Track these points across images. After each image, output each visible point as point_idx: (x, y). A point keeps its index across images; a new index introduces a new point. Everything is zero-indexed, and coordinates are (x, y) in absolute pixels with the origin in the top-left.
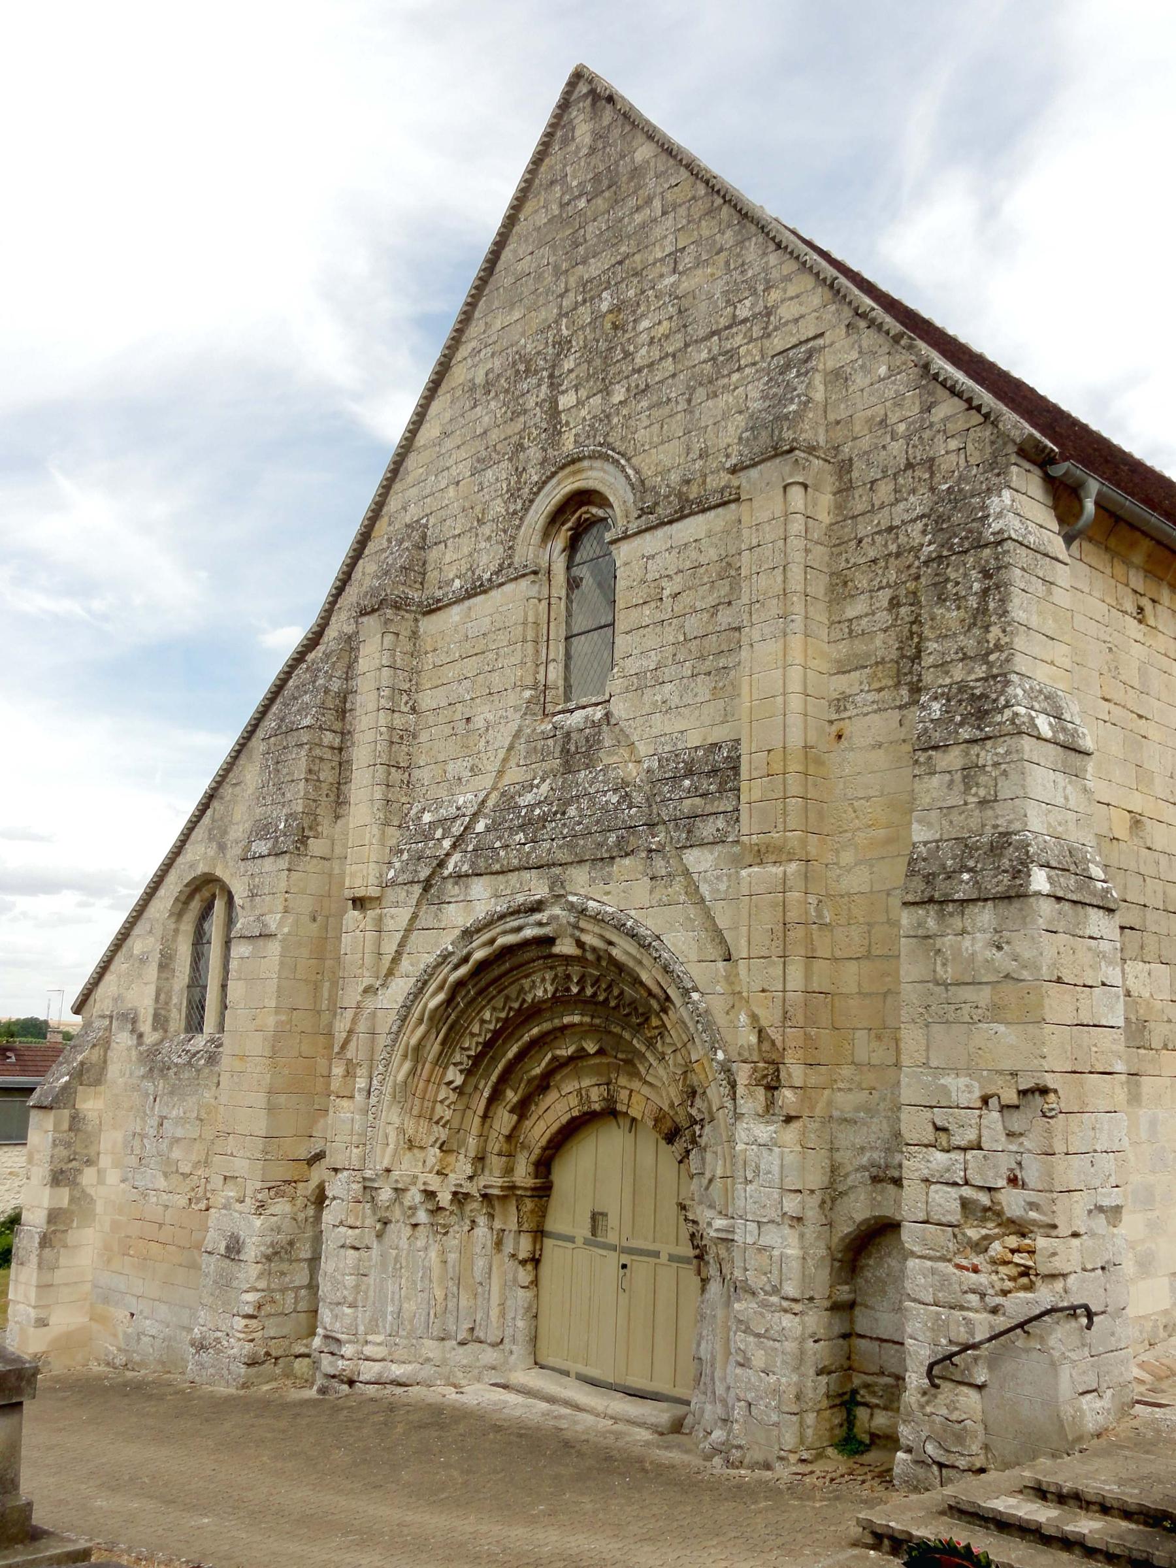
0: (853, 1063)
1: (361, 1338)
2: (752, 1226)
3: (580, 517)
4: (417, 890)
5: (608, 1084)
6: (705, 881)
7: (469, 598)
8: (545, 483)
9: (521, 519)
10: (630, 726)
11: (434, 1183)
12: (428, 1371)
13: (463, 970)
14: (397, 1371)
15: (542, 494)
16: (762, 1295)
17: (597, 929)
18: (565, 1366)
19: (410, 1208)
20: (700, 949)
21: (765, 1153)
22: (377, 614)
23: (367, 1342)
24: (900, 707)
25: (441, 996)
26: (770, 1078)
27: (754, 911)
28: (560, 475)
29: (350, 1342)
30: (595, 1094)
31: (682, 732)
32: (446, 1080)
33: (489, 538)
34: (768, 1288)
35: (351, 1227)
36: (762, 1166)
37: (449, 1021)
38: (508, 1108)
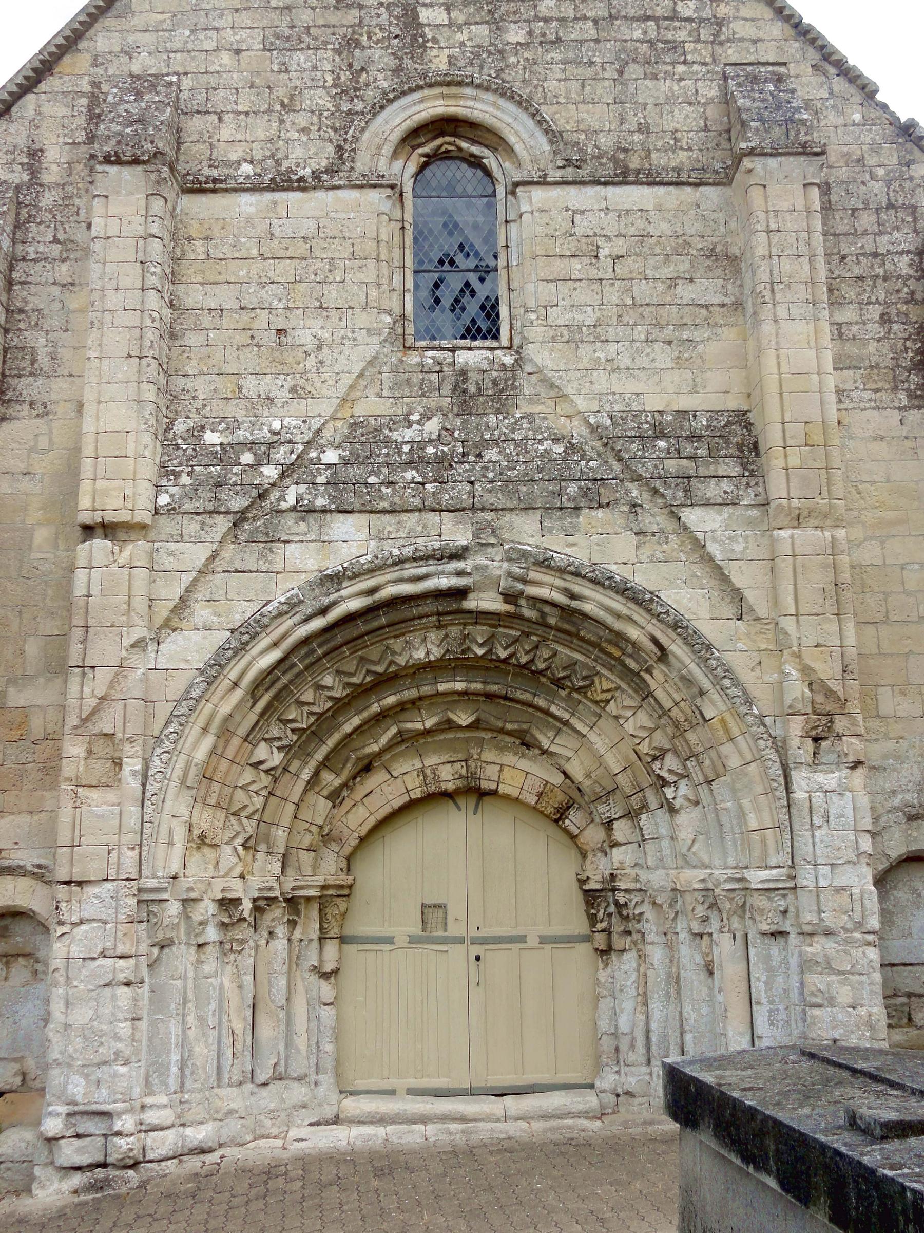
0: (879, 716)
1: (137, 1104)
3: (441, 146)
4: (223, 524)
5: (466, 761)
6: (714, 540)
7: (273, 190)
8: (404, 93)
9: (366, 123)
10: (561, 377)
11: (237, 889)
12: (233, 1127)
13: (318, 623)
14: (198, 1135)
15: (396, 105)
16: (844, 935)
17: (559, 582)
18: (385, 1085)
19: (201, 924)
20: (712, 606)
21: (835, 798)
22: (140, 168)
23: (143, 1107)
24: (899, 409)
25: (275, 655)
26: (820, 729)
28: (426, 92)
29: (125, 1112)
30: (446, 773)
31: (637, 394)
32: (254, 759)
33: (305, 130)
34: (849, 926)
35: (121, 957)
37: (278, 686)
38: (325, 793)
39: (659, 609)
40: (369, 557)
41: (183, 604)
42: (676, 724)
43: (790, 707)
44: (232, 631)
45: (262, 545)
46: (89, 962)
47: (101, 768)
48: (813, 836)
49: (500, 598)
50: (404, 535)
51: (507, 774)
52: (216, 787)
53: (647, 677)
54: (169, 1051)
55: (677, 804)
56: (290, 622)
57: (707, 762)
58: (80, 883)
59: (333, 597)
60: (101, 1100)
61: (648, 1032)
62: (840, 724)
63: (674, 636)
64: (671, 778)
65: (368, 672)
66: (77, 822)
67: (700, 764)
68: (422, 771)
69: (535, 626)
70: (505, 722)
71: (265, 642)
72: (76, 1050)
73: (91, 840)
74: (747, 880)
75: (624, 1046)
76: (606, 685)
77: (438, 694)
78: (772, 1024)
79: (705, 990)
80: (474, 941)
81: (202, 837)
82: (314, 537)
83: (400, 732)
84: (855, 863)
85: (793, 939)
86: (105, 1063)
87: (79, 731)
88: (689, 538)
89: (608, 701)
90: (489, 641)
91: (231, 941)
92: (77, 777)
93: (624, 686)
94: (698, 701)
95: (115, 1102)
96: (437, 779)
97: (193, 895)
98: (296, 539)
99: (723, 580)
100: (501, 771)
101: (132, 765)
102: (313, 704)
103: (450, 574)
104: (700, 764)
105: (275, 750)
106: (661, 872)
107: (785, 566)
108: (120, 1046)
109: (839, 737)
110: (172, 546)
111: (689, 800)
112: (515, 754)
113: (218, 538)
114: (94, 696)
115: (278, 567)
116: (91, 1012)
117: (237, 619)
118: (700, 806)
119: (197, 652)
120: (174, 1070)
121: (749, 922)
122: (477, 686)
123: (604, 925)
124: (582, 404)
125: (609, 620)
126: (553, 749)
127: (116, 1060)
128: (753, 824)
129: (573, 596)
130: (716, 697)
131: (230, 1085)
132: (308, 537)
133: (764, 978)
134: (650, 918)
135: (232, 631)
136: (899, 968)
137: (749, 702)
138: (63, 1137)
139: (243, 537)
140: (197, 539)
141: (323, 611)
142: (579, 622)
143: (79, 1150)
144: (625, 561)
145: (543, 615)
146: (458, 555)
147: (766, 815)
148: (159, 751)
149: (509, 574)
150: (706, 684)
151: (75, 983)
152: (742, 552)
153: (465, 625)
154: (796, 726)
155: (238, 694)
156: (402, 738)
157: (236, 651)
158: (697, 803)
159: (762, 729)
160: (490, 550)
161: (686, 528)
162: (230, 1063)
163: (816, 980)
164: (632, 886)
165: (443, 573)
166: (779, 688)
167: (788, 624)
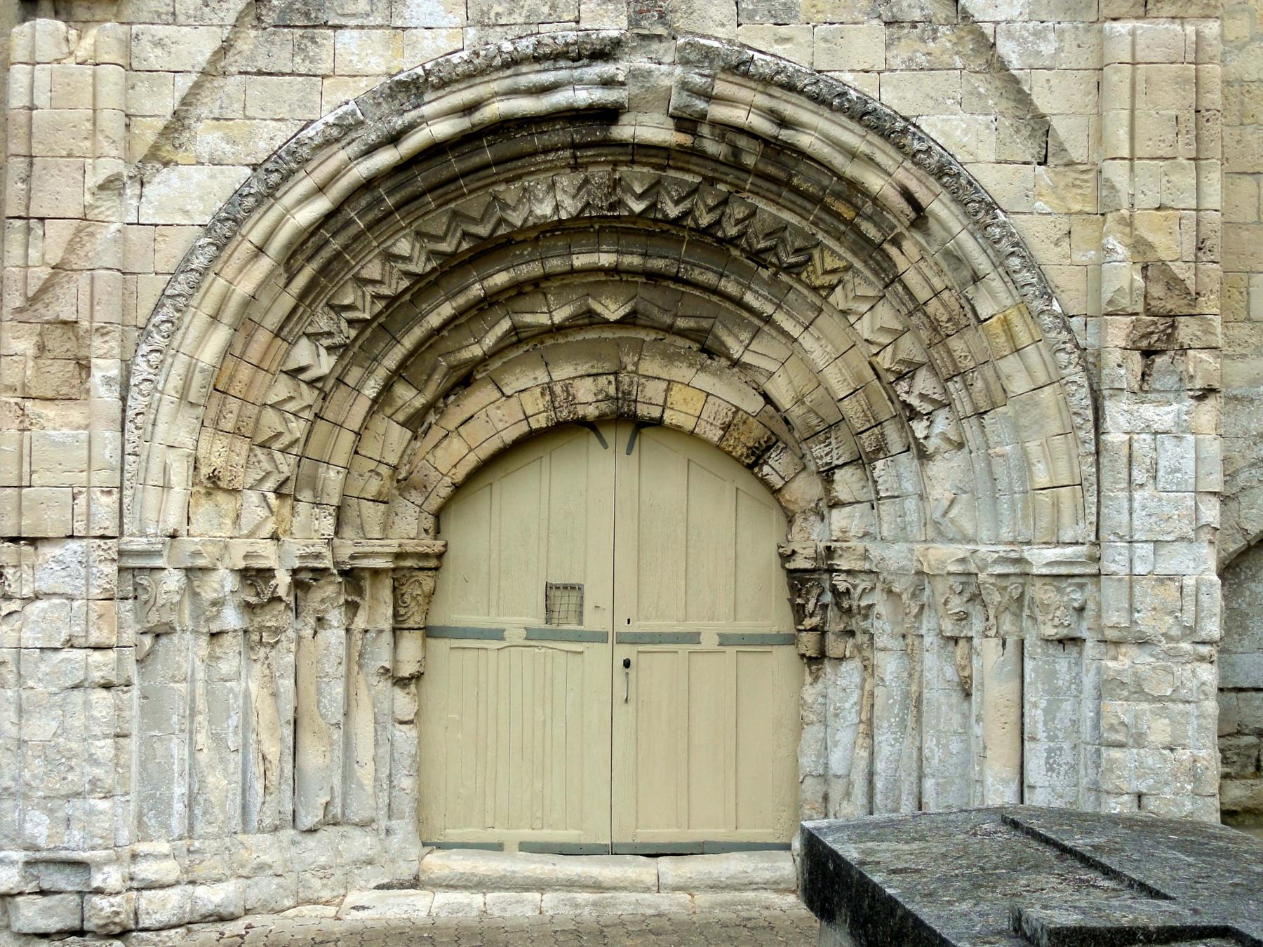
0: (1249, 319)
1: (126, 853)
2: (1144, 550)
5: (616, 373)
6: (1010, 35)
11: (268, 555)
12: (265, 887)
13: (386, 158)
14: (212, 896)
16: (1164, 645)
17: (761, 100)
19: (214, 604)
20: (1000, 142)
21: (1169, 443)
23: (134, 856)
25: (321, 206)
26: (1155, 337)
27: (1141, 87)
29: (108, 862)
32: (292, 365)
34: (1175, 632)
35: (96, 648)
36: (1163, 463)
37: (326, 254)
38: (401, 417)
39: (917, 146)
40: (465, 55)
41: (177, 124)
42: (935, 326)
43: (1110, 302)
44: (255, 167)
45: (299, 32)
46: (49, 653)
47: (59, 373)
48: (1131, 500)
49: (670, 123)
50: (521, 20)
51: (677, 394)
52: (233, 405)
53: (893, 251)
54: (171, 782)
55: (931, 445)
56: (342, 155)
57: (979, 385)
58: (33, 541)
59: (409, 117)
60: (72, 845)
61: (871, 775)
62: (1187, 331)
63: (937, 188)
64: (925, 408)
65: (465, 235)
66: (26, 451)
67: (968, 387)
68: (548, 388)
69: (723, 169)
70: (676, 316)
71: (304, 185)
72: (34, 777)
73: (48, 478)
74: (1027, 562)
75: (836, 792)
76: (830, 263)
77: (573, 271)
78: (1051, 769)
79: (957, 719)
80: (622, 639)
81: (214, 479)
82: (380, 21)
83: (514, 329)
84: (1191, 541)
85: (1090, 648)
86: (78, 794)
87: (24, 317)
88: (971, 32)
89: (832, 288)
90: (653, 190)
91: (261, 630)
92: (24, 385)
93: (858, 264)
94: (970, 293)
95: (93, 848)
96: (571, 400)
97: (201, 562)
98: (353, 22)
99: (1020, 101)
100: (668, 390)
101: (105, 368)
102: (381, 282)
103: (592, 83)
104: (968, 387)
105: (323, 352)
106: (901, 547)
107: (1118, 79)
108: (98, 772)
109: (1184, 350)
110: (160, 31)
111: (949, 440)
112: (691, 365)
113: (231, 19)
114: (45, 264)
115: (324, 68)
116: (54, 724)
117: (262, 149)
118: (966, 450)
119: (201, 199)
120: (178, 807)
121: (1026, 623)
122: (632, 260)
123: (815, 621)
125: (838, 160)
126: (748, 358)
127: (92, 791)
128: (1042, 478)
129: (783, 123)
130: (997, 284)
131: (261, 830)
132: (371, 21)
133: (1043, 704)
134: (883, 612)
135: (255, 167)
136: (1249, 694)
137: (1047, 294)
138: (21, 894)
139: (271, 17)
140: (198, 21)
141: (394, 139)
142: (791, 163)
143: (45, 911)
144: (866, 67)
145: (736, 151)
146: (605, 53)
147: (1062, 466)
148: (145, 349)
149: (684, 86)
150: (983, 263)
151: (31, 683)
152: (1053, 57)
153: (615, 164)
154: (1118, 333)
155: (265, 264)
156: (518, 337)
157: (260, 199)
158: (961, 446)
159: (1064, 335)
160: (655, 46)
161: (966, 16)
162: (260, 800)
163: (1117, 709)
164: (858, 565)
165: (580, 81)
166: (1095, 274)
167: (1117, 173)
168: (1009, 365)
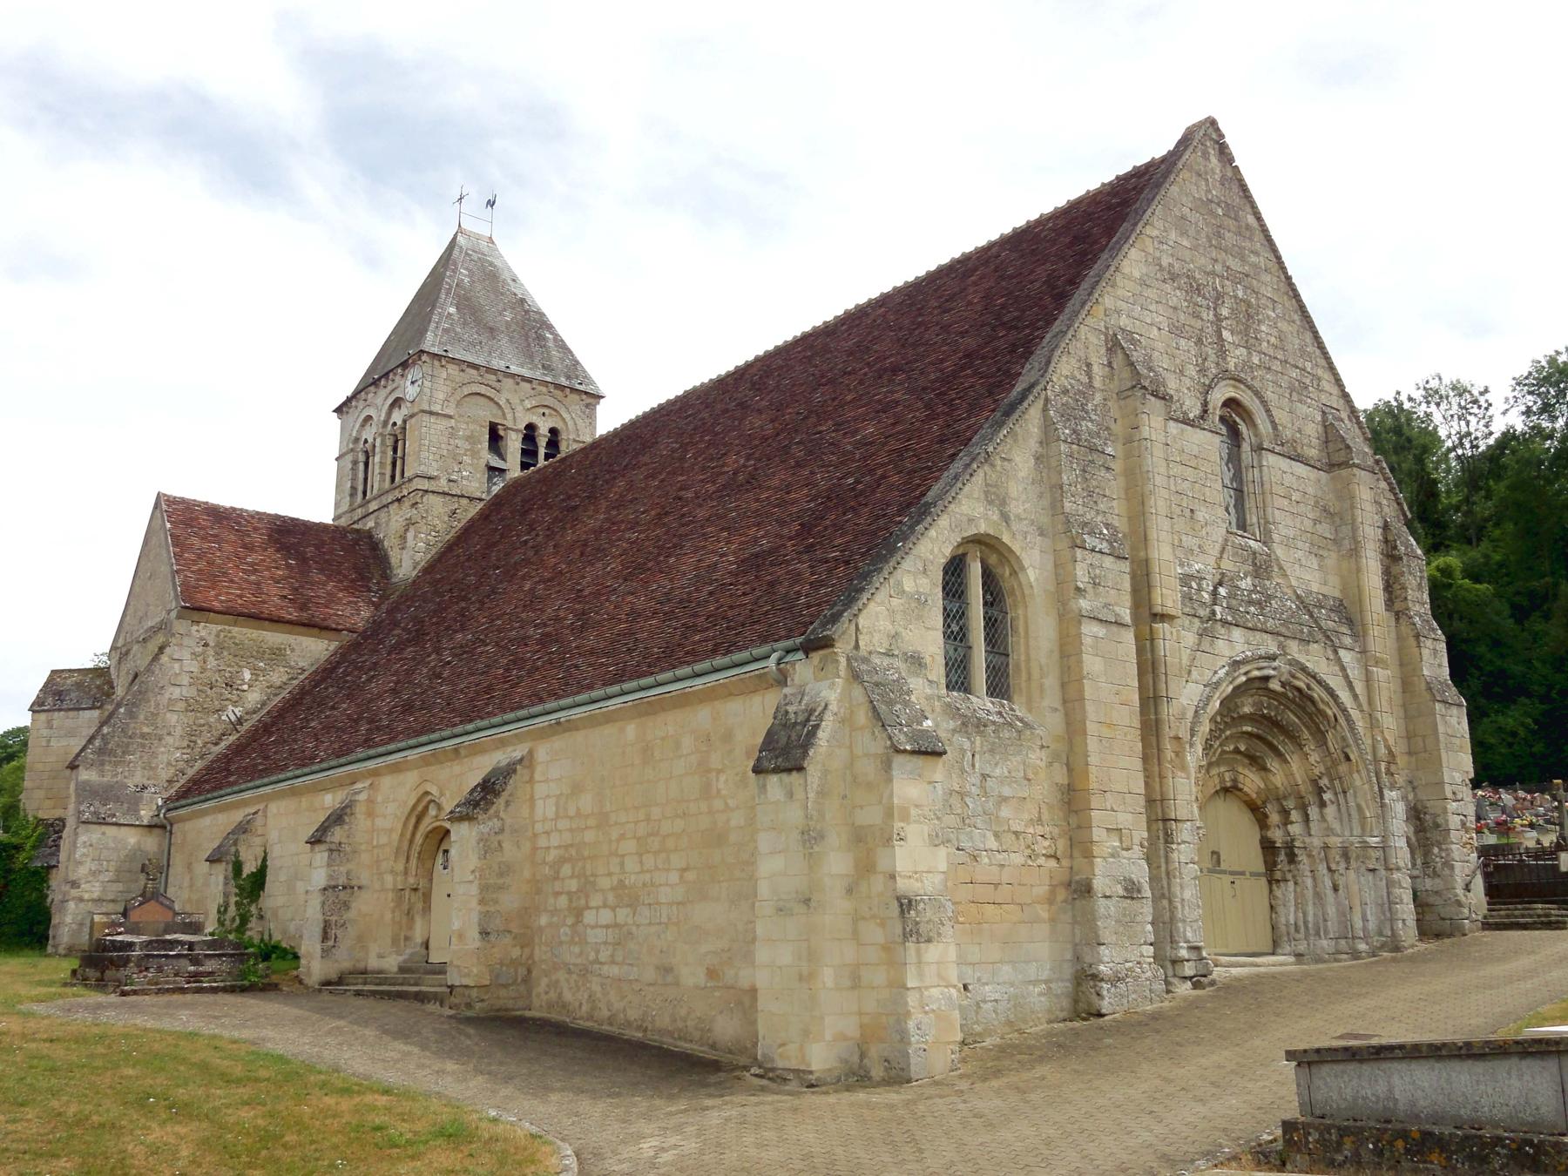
30: (1227, 777)
67: (1342, 784)
94: (1347, 750)
124: (1294, 583)
149: (1290, 673)
161: (1339, 659)
168: (1355, 775)
